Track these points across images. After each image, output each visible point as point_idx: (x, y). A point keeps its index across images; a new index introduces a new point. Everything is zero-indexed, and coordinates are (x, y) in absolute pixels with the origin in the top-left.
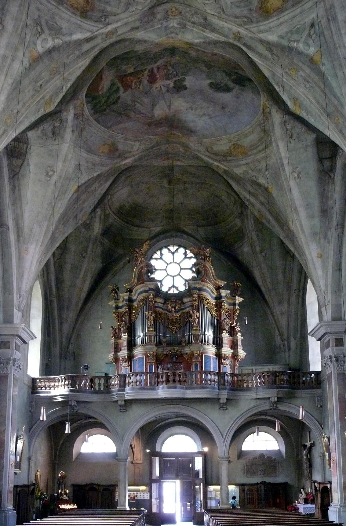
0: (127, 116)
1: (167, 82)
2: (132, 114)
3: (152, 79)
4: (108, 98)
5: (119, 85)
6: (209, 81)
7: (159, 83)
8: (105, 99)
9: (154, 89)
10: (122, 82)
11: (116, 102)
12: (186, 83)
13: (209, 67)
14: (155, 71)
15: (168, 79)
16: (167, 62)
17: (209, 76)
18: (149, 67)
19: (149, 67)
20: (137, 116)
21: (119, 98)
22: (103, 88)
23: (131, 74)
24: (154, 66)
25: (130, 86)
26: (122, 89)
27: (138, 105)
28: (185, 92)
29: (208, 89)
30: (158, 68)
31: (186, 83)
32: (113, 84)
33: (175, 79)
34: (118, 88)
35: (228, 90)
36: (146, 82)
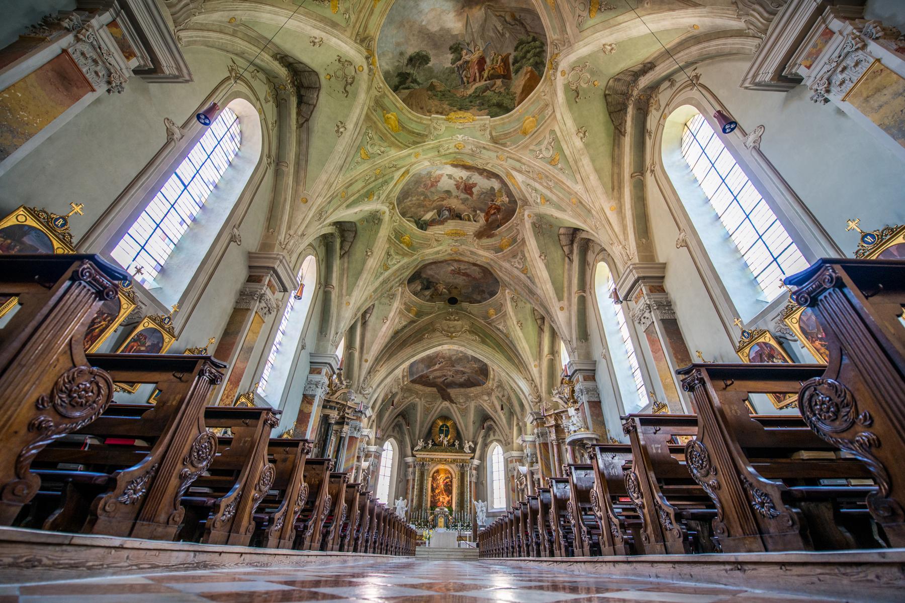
0: (513, 17)
1: (467, 58)
2: (508, 18)
3: (481, 61)
4: (524, 57)
5: (511, 68)
6: (430, 64)
7: (475, 57)
8: (529, 55)
9: (481, 49)
10: (508, 70)
11: (521, 43)
12: (451, 56)
13: (432, 87)
14: (477, 75)
15: (467, 62)
16: (467, 89)
17: (431, 70)
18: (483, 83)
19: (483, 83)
20: (503, 14)
21: (516, 49)
22: (526, 74)
23: (498, 77)
24: (477, 85)
25: (502, 60)
26: (511, 60)
27: (500, 29)
28: (452, 43)
29: (431, 53)
30: (475, 80)
31: (451, 56)
32: (517, 71)
33: (461, 62)
34: (513, 64)
35: (411, 60)
36: (488, 60)
